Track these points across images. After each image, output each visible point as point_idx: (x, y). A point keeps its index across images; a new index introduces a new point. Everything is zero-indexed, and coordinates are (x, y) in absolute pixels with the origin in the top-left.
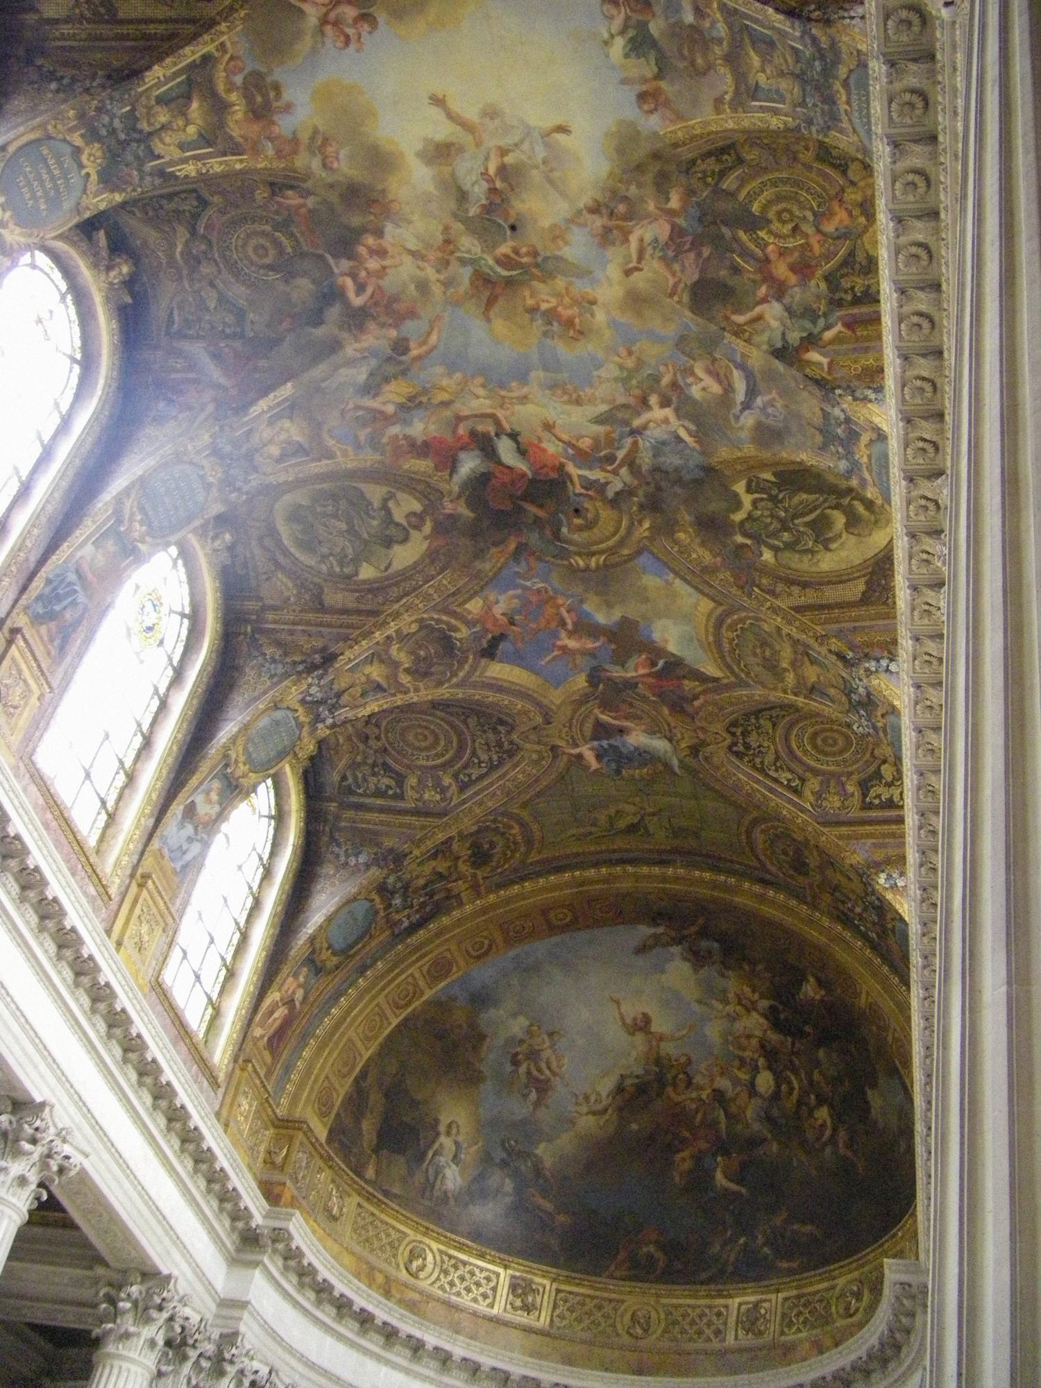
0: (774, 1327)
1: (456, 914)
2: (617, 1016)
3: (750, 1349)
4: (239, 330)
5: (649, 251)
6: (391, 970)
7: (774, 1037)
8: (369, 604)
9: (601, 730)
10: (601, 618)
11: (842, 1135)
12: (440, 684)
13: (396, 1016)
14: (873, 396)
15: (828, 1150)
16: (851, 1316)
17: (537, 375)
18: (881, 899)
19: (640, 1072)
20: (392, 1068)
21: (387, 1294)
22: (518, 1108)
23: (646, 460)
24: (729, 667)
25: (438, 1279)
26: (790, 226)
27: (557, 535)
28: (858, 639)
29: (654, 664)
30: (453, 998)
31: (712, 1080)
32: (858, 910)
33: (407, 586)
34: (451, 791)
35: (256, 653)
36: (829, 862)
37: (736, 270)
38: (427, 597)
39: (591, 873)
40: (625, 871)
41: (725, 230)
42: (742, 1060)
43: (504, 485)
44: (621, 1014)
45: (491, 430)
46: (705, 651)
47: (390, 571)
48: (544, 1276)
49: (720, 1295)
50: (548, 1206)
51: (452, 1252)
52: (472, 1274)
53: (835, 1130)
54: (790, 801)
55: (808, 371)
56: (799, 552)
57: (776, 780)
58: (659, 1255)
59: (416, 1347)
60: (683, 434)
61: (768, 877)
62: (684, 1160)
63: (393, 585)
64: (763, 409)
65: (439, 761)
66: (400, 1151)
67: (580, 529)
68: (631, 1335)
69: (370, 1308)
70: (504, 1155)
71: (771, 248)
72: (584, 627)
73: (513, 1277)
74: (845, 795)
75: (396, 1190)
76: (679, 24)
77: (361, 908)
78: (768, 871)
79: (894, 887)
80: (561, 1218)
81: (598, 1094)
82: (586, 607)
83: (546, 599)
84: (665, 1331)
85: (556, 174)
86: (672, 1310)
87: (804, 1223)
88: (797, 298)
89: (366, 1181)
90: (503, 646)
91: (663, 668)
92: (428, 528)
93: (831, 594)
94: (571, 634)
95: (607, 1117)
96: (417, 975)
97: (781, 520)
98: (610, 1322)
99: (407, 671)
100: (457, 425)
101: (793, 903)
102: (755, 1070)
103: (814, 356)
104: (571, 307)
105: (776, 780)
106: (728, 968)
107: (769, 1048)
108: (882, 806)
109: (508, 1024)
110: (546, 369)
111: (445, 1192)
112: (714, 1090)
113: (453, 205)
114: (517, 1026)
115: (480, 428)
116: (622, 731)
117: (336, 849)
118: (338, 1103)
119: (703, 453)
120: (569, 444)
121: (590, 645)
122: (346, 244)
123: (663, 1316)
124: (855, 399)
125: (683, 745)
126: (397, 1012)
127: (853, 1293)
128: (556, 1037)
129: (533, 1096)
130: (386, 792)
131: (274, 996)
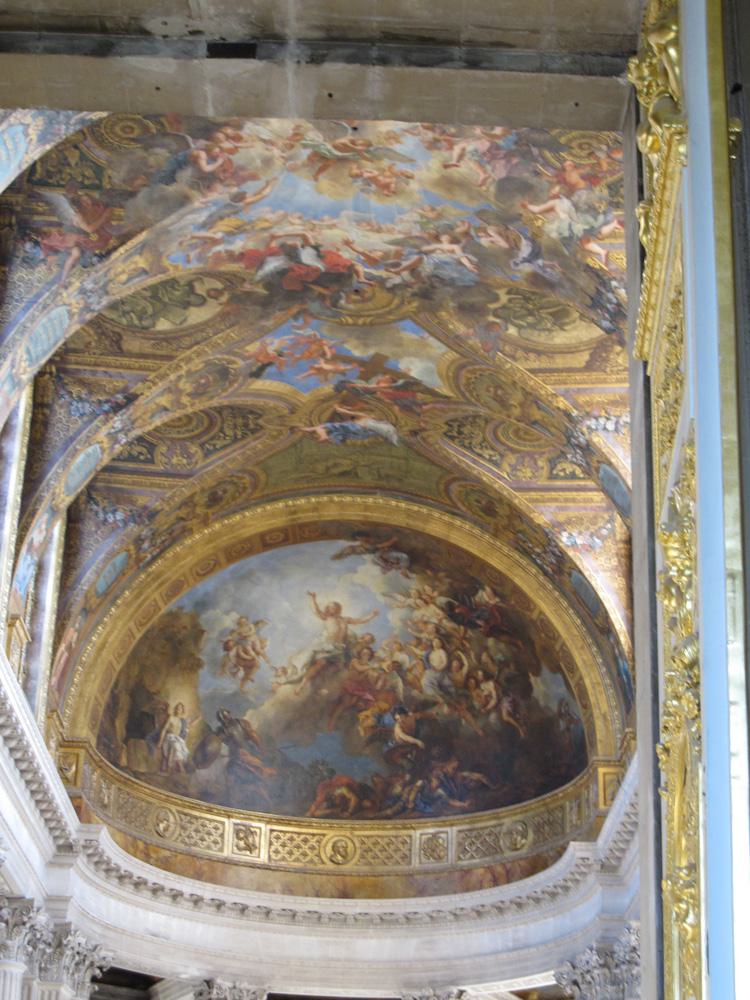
1: (188, 542)
3: (434, 872)
4: (97, 182)
5: (468, 156)
6: (137, 597)
7: (448, 624)
9: (335, 417)
10: (357, 353)
11: (506, 706)
12: (212, 398)
15: (493, 717)
16: (517, 849)
17: (347, 214)
18: (563, 553)
19: (330, 647)
20: (135, 670)
21: (147, 858)
22: (228, 685)
23: (427, 268)
24: (461, 392)
26: (587, 152)
27: (335, 304)
28: (582, 399)
29: (395, 381)
30: (181, 608)
31: (392, 654)
32: (538, 550)
33: (199, 337)
34: (197, 457)
35: (62, 392)
36: (516, 514)
37: (537, 173)
38: (216, 346)
39: (302, 501)
40: (332, 501)
41: (535, 151)
42: (419, 642)
43: (300, 275)
44: (316, 604)
45: (299, 242)
46: (443, 380)
49: (405, 828)
50: (256, 761)
51: (187, 811)
52: (204, 826)
53: (499, 701)
54: (490, 471)
56: (540, 330)
57: (480, 455)
59: (176, 896)
60: (464, 261)
61: (456, 511)
62: (367, 718)
64: (543, 268)
65: (187, 435)
66: (143, 736)
67: (355, 302)
69: (144, 876)
70: (219, 724)
71: (568, 163)
72: (341, 357)
73: (235, 824)
74: (536, 468)
75: (143, 769)
77: (119, 559)
79: (574, 545)
80: (268, 771)
81: (295, 667)
82: (347, 346)
83: (312, 340)
84: (362, 857)
86: (365, 840)
87: (475, 768)
88: (584, 198)
89: (122, 769)
90: (268, 370)
92: (224, 298)
93: (560, 362)
94: (327, 361)
95: (302, 684)
98: (316, 852)
99: (189, 395)
101: (477, 531)
102: (431, 648)
103: (593, 246)
104: (390, 177)
105: (480, 455)
106: (412, 571)
110: (356, 209)
111: (177, 764)
112: (394, 662)
114: (229, 621)
116: (353, 418)
117: (95, 507)
118: (101, 713)
119: (480, 275)
120: (363, 254)
121: (342, 367)
123: (358, 845)
125: (405, 429)
129: (241, 673)
131: (63, 647)
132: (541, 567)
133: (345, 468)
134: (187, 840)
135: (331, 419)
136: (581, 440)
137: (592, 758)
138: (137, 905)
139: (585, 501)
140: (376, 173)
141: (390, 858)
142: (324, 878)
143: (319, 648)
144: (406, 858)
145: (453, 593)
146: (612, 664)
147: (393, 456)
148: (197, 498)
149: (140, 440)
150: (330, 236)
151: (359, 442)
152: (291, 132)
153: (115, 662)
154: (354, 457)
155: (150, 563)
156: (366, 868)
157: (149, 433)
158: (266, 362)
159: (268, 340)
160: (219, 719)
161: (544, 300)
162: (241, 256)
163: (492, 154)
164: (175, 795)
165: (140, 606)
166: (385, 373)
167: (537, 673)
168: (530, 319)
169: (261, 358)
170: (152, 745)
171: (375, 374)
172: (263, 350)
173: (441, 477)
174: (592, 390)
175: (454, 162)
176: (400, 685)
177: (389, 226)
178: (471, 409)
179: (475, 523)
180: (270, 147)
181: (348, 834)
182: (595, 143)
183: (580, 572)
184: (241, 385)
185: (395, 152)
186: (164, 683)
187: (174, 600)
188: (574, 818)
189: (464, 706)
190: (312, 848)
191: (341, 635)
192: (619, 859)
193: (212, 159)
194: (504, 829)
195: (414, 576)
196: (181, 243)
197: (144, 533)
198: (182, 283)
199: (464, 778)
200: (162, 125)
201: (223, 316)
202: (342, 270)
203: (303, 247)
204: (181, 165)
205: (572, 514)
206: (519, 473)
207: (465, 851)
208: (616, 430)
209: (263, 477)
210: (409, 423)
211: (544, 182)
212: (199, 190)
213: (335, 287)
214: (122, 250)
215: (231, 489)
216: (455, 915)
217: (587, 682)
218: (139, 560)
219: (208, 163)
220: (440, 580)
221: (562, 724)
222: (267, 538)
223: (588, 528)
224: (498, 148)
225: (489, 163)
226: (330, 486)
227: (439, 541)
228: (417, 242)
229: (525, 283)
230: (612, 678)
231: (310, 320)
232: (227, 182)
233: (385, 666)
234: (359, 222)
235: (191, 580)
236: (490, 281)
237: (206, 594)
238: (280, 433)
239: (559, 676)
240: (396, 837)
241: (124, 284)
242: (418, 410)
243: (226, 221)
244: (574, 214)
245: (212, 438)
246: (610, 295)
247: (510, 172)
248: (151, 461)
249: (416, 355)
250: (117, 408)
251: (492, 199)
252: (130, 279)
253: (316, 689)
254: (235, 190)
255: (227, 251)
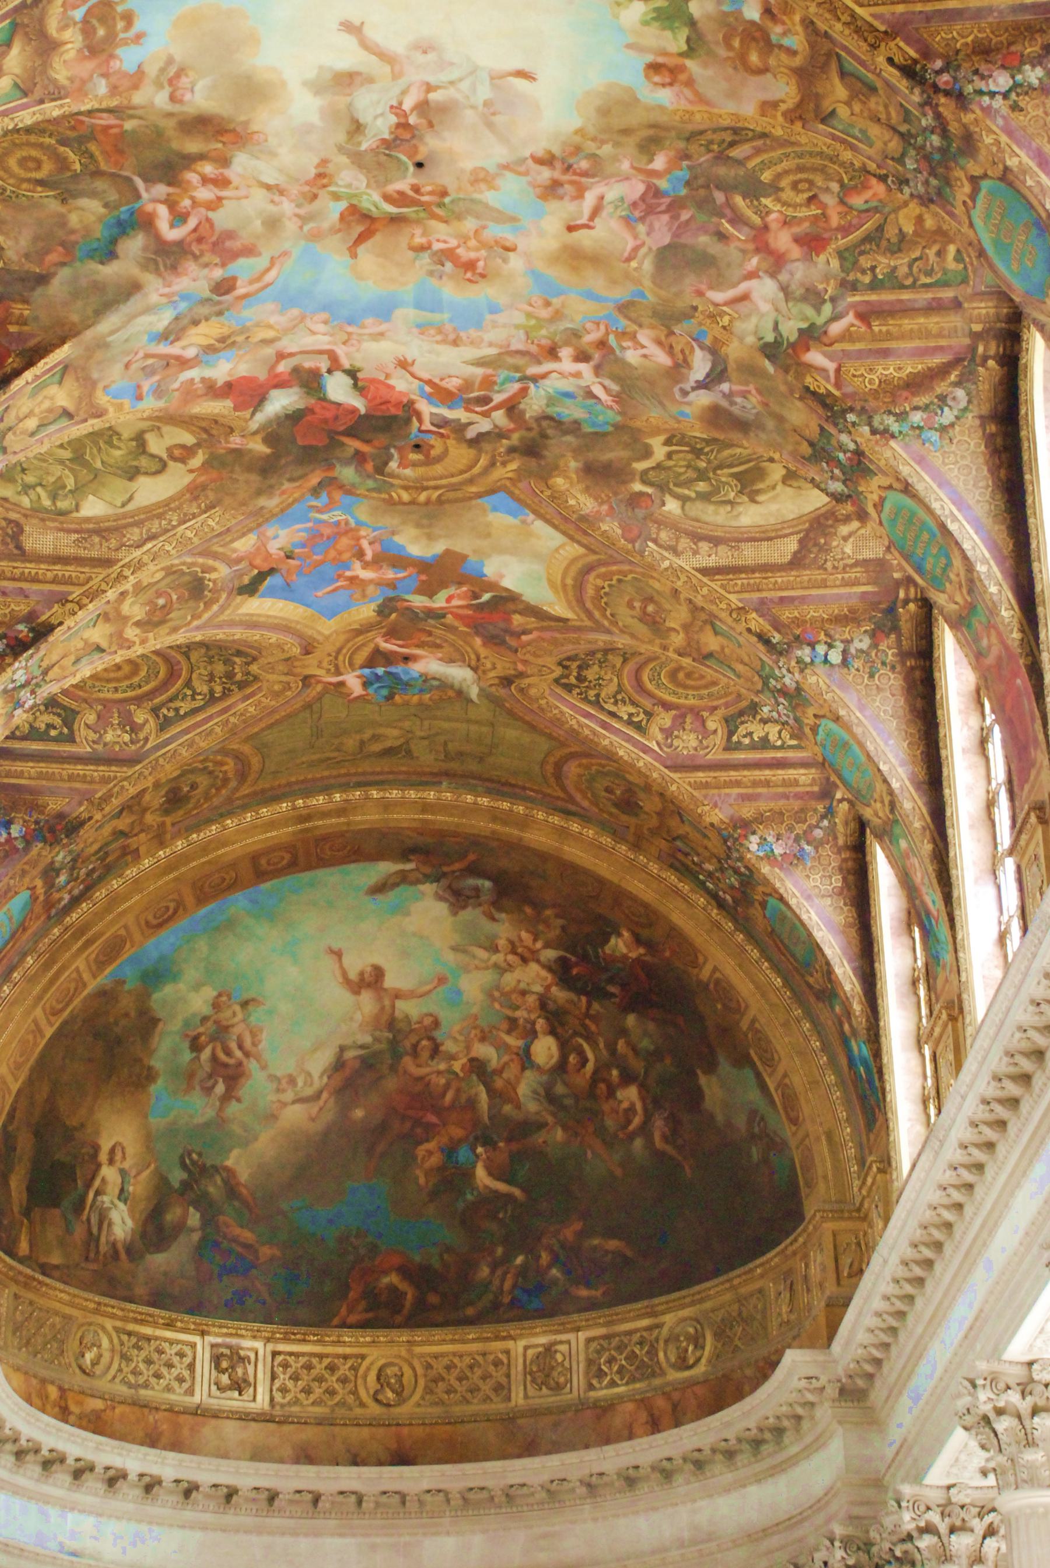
0: (578, 1380)
1: (131, 872)
2: (338, 973)
3: (548, 1411)
5: (608, 210)
6: (47, 966)
7: (560, 995)
8: (96, 549)
10: (416, 550)
11: (659, 1125)
12: (175, 630)
13: (51, 1025)
14: (895, 428)
15: (638, 1143)
17: (406, 314)
19: (368, 1039)
21: (63, 1414)
22: (198, 1108)
23: (535, 403)
25: (120, 1370)
26: (806, 195)
27: (380, 469)
28: (786, 614)
29: (476, 596)
31: (468, 1048)
33: (155, 526)
36: (672, 809)
37: (722, 237)
38: (183, 541)
40: (367, 798)
41: (719, 197)
42: (513, 1023)
43: (325, 421)
44: (341, 967)
45: (324, 364)
47: (130, 507)
48: (254, 1337)
49: (497, 1338)
51: (131, 1327)
52: (160, 1352)
54: (629, 739)
55: (808, 380)
58: (404, 1286)
59: (114, 1479)
60: (598, 390)
61: (573, 808)
62: (429, 1154)
63: (132, 525)
64: (729, 396)
65: (130, 694)
66: (55, 1203)
67: (414, 464)
68: (377, 1401)
70: (185, 1176)
71: (773, 216)
73: (213, 1346)
74: (705, 733)
75: (56, 1259)
76: (738, 14)
78: (577, 804)
79: (770, 857)
81: (309, 1074)
82: (398, 539)
83: (342, 530)
84: (428, 1390)
85: (498, 119)
88: (798, 275)
89: (21, 1261)
91: (488, 602)
92: (197, 461)
93: (749, 554)
94: (366, 565)
95: (321, 1102)
96: (82, 967)
97: (697, 469)
98: (350, 1386)
99: (138, 624)
100: (277, 362)
101: (606, 840)
102: (532, 1034)
103: (815, 357)
104: (477, 249)
106: (500, 909)
107: (551, 1006)
108: (753, 747)
109: (187, 999)
110: (419, 305)
111: (114, 1245)
112: (472, 1060)
113: (341, 137)
114: (199, 1002)
115: (308, 364)
116: (406, 659)
120: (429, 382)
121: (390, 574)
122: (170, 169)
123: (420, 1371)
124: (874, 432)
125: (492, 674)
126: (53, 1019)
127: (689, 1338)
128: (250, 1008)
129: (220, 1088)
130: (47, 732)
132: (714, 896)
133: (388, 744)
134: (132, 1379)
135: (370, 663)
136: (787, 680)
137: (810, 1207)
138: (46, 1500)
139: (785, 783)
140: (453, 243)
141: (474, 1390)
142: (365, 1432)
143: (348, 1042)
144: (502, 1389)
145: (566, 942)
146: (839, 1050)
147: (469, 721)
148: (147, 797)
149: (51, 704)
150: (374, 354)
151: (415, 699)
152: (313, 172)
153: (9, 1079)
154: (407, 724)
155: (67, 910)
156: (437, 1411)
157: (65, 692)
158: (266, 567)
159: (270, 532)
160: (184, 1166)
161: (726, 453)
162: (229, 389)
163: (649, 204)
164: (113, 1302)
165: (52, 982)
166: (460, 584)
167: (711, 1068)
168: (702, 486)
169: (258, 561)
170: (70, 1217)
171: (443, 585)
172: (261, 547)
173: (549, 754)
174: (803, 599)
175: (583, 221)
176: (483, 1096)
177: (473, 333)
178: (601, 639)
179: (603, 826)
180: (277, 198)
181: (404, 1353)
182: (819, 180)
183: (781, 899)
184: (223, 609)
185: (486, 206)
186: (91, 1111)
187: (108, 971)
188: (785, 1309)
189: (591, 1130)
190: (344, 1381)
191: (384, 1018)
192: (870, 1377)
193: (179, 217)
194: (665, 1331)
195: (503, 916)
196: (127, 366)
197: (60, 857)
198: (125, 435)
199: (595, 1248)
200: (92, 156)
201: (194, 491)
202: (393, 411)
203: (329, 371)
204: (123, 228)
205: (763, 805)
206: (676, 743)
207: (600, 1374)
208: (845, 662)
209: (255, 762)
210: (500, 664)
211: (732, 251)
212: (157, 272)
213: (382, 439)
214: (28, 375)
215: (203, 781)
216: (589, 1485)
217: (797, 1081)
218: (49, 904)
219: (172, 226)
220: (546, 923)
221: (755, 1153)
222: (263, 861)
223: (791, 829)
224: (658, 193)
225: (642, 219)
226: (364, 774)
227: (543, 857)
228: (520, 361)
229: (698, 425)
230: (838, 1072)
231: (338, 495)
232: (206, 259)
233: (457, 1066)
234: (422, 328)
235: (137, 936)
236: (638, 424)
237: (162, 958)
238: (287, 686)
239: (748, 1073)
240: (484, 1354)
241: (32, 434)
242: (512, 642)
243: (203, 328)
244: (782, 305)
245: (171, 700)
246: (844, 438)
247: (676, 235)
248: (71, 739)
249: (513, 551)
250: (18, 647)
251: (647, 283)
252: (41, 426)
253: (344, 1110)
254: (218, 273)
255: (203, 380)
